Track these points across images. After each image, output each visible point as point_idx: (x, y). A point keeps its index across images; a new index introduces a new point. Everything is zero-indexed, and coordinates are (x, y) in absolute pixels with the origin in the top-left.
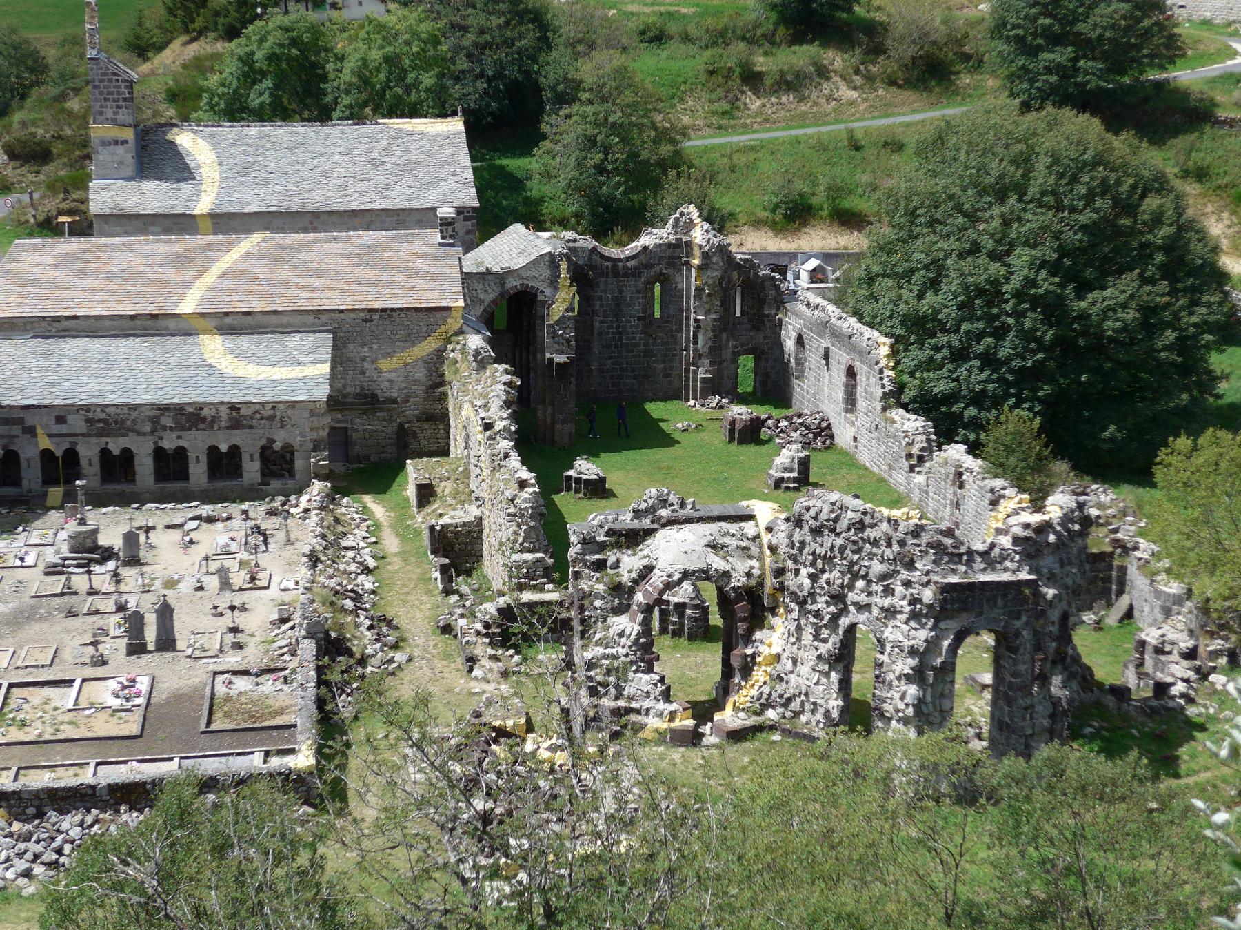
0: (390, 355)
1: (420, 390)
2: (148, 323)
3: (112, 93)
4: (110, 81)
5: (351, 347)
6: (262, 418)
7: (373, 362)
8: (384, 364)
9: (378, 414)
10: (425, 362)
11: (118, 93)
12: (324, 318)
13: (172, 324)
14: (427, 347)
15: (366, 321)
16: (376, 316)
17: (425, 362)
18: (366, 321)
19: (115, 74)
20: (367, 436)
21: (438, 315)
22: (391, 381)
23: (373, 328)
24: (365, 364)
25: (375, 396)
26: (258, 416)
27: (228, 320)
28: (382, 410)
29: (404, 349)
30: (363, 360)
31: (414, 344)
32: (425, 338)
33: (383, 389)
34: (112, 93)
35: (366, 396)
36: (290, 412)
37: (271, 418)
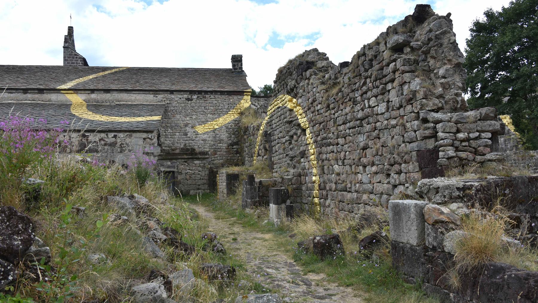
0: (204, 122)
1: (224, 146)
2: (37, 96)
3: (74, 63)
4: (73, 58)
5: (178, 116)
6: (105, 145)
7: (192, 127)
8: (200, 129)
9: (197, 162)
10: (227, 127)
11: (77, 63)
12: (160, 97)
13: (54, 97)
14: (229, 118)
15: (188, 99)
16: (195, 97)
17: (227, 127)
18: (188, 99)
19: (76, 55)
20: (188, 177)
21: (235, 97)
22: (204, 140)
23: (193, 104)
24: (187, 128)
25: (194, 150)
26: (103, 142)
27: (93, 96)
28: (198, 159)
29: (213, 119)
30: (186, 125)
31: (219, 116)
32: (227, 113)
33: (198, 146)
34: (74, 63)
35: (188, 150)
36: (128, 140)
37: (113, 145)
